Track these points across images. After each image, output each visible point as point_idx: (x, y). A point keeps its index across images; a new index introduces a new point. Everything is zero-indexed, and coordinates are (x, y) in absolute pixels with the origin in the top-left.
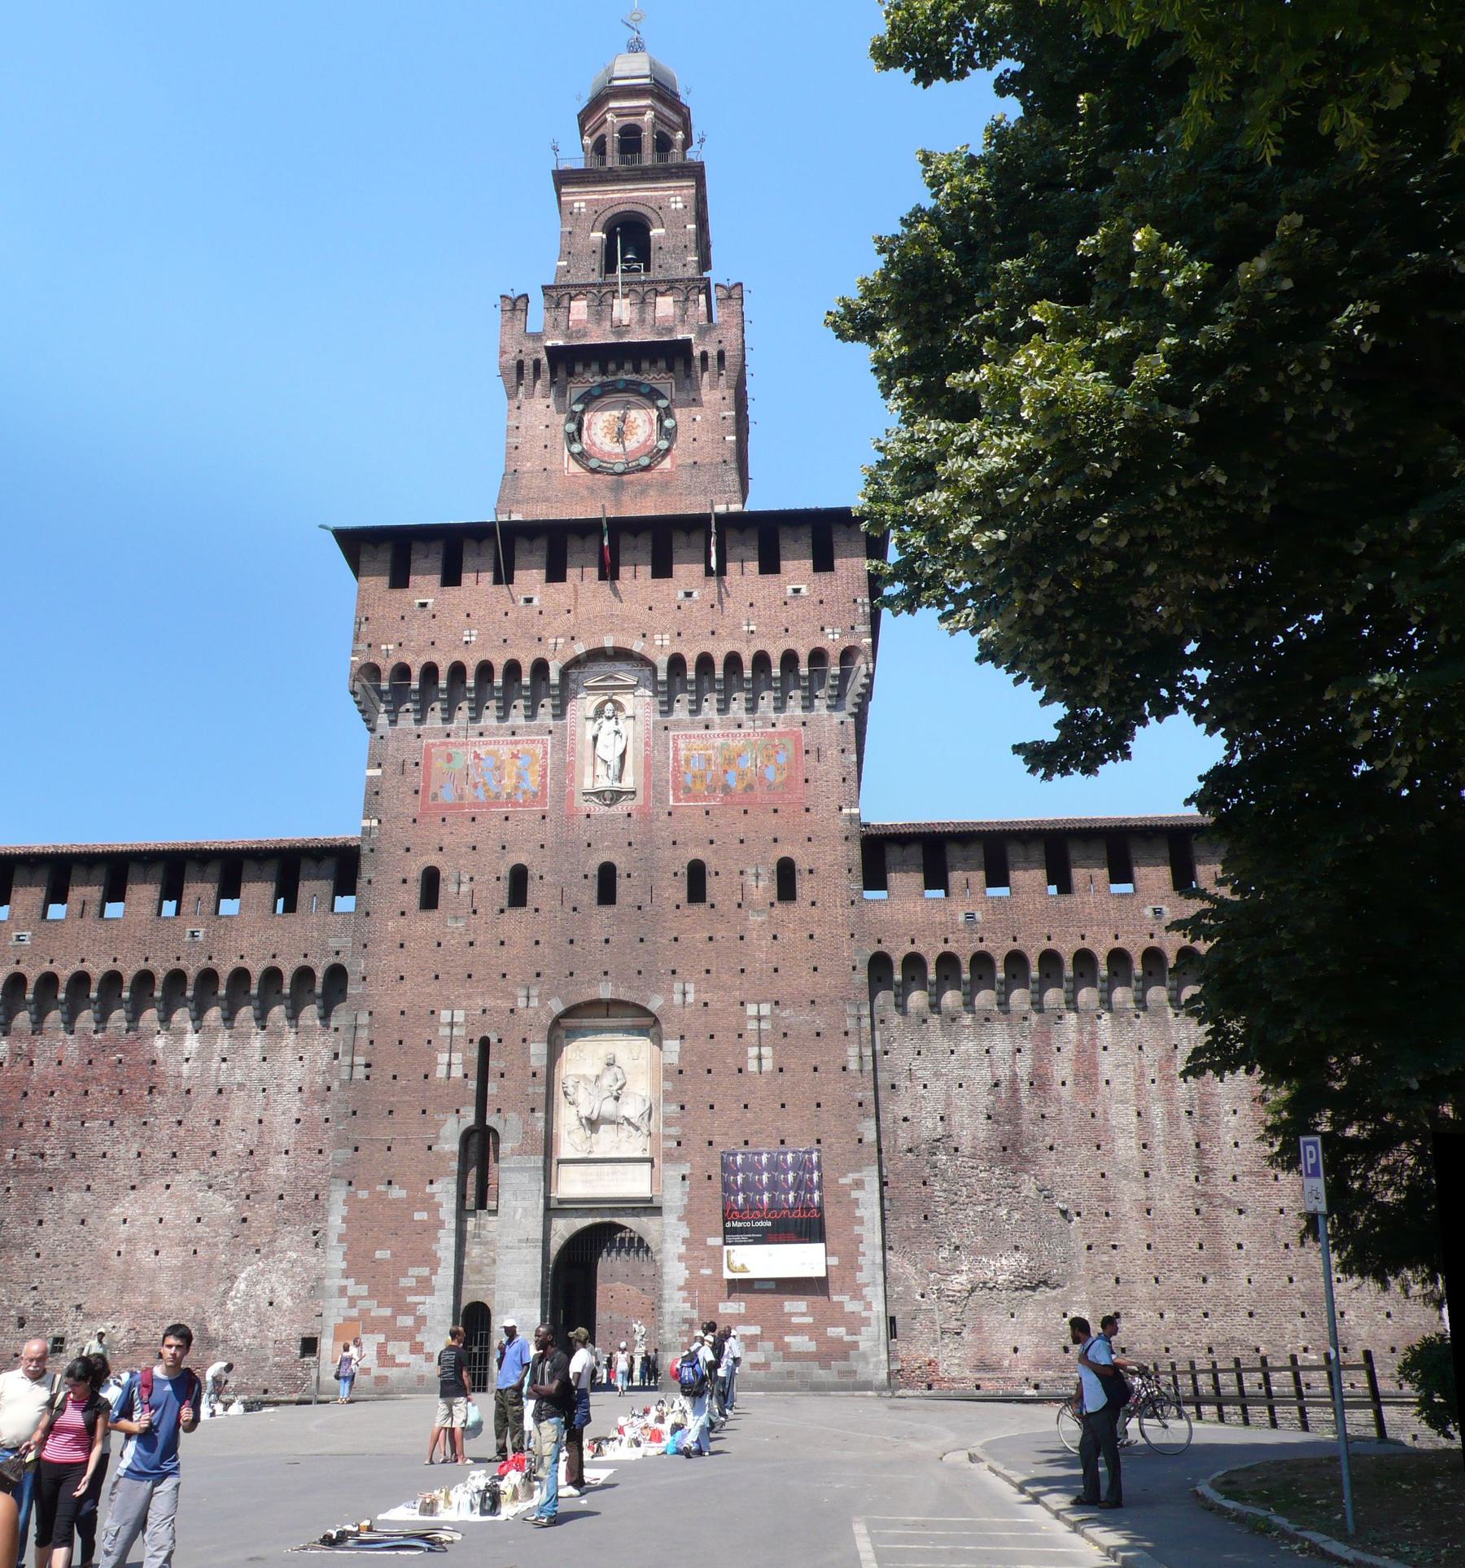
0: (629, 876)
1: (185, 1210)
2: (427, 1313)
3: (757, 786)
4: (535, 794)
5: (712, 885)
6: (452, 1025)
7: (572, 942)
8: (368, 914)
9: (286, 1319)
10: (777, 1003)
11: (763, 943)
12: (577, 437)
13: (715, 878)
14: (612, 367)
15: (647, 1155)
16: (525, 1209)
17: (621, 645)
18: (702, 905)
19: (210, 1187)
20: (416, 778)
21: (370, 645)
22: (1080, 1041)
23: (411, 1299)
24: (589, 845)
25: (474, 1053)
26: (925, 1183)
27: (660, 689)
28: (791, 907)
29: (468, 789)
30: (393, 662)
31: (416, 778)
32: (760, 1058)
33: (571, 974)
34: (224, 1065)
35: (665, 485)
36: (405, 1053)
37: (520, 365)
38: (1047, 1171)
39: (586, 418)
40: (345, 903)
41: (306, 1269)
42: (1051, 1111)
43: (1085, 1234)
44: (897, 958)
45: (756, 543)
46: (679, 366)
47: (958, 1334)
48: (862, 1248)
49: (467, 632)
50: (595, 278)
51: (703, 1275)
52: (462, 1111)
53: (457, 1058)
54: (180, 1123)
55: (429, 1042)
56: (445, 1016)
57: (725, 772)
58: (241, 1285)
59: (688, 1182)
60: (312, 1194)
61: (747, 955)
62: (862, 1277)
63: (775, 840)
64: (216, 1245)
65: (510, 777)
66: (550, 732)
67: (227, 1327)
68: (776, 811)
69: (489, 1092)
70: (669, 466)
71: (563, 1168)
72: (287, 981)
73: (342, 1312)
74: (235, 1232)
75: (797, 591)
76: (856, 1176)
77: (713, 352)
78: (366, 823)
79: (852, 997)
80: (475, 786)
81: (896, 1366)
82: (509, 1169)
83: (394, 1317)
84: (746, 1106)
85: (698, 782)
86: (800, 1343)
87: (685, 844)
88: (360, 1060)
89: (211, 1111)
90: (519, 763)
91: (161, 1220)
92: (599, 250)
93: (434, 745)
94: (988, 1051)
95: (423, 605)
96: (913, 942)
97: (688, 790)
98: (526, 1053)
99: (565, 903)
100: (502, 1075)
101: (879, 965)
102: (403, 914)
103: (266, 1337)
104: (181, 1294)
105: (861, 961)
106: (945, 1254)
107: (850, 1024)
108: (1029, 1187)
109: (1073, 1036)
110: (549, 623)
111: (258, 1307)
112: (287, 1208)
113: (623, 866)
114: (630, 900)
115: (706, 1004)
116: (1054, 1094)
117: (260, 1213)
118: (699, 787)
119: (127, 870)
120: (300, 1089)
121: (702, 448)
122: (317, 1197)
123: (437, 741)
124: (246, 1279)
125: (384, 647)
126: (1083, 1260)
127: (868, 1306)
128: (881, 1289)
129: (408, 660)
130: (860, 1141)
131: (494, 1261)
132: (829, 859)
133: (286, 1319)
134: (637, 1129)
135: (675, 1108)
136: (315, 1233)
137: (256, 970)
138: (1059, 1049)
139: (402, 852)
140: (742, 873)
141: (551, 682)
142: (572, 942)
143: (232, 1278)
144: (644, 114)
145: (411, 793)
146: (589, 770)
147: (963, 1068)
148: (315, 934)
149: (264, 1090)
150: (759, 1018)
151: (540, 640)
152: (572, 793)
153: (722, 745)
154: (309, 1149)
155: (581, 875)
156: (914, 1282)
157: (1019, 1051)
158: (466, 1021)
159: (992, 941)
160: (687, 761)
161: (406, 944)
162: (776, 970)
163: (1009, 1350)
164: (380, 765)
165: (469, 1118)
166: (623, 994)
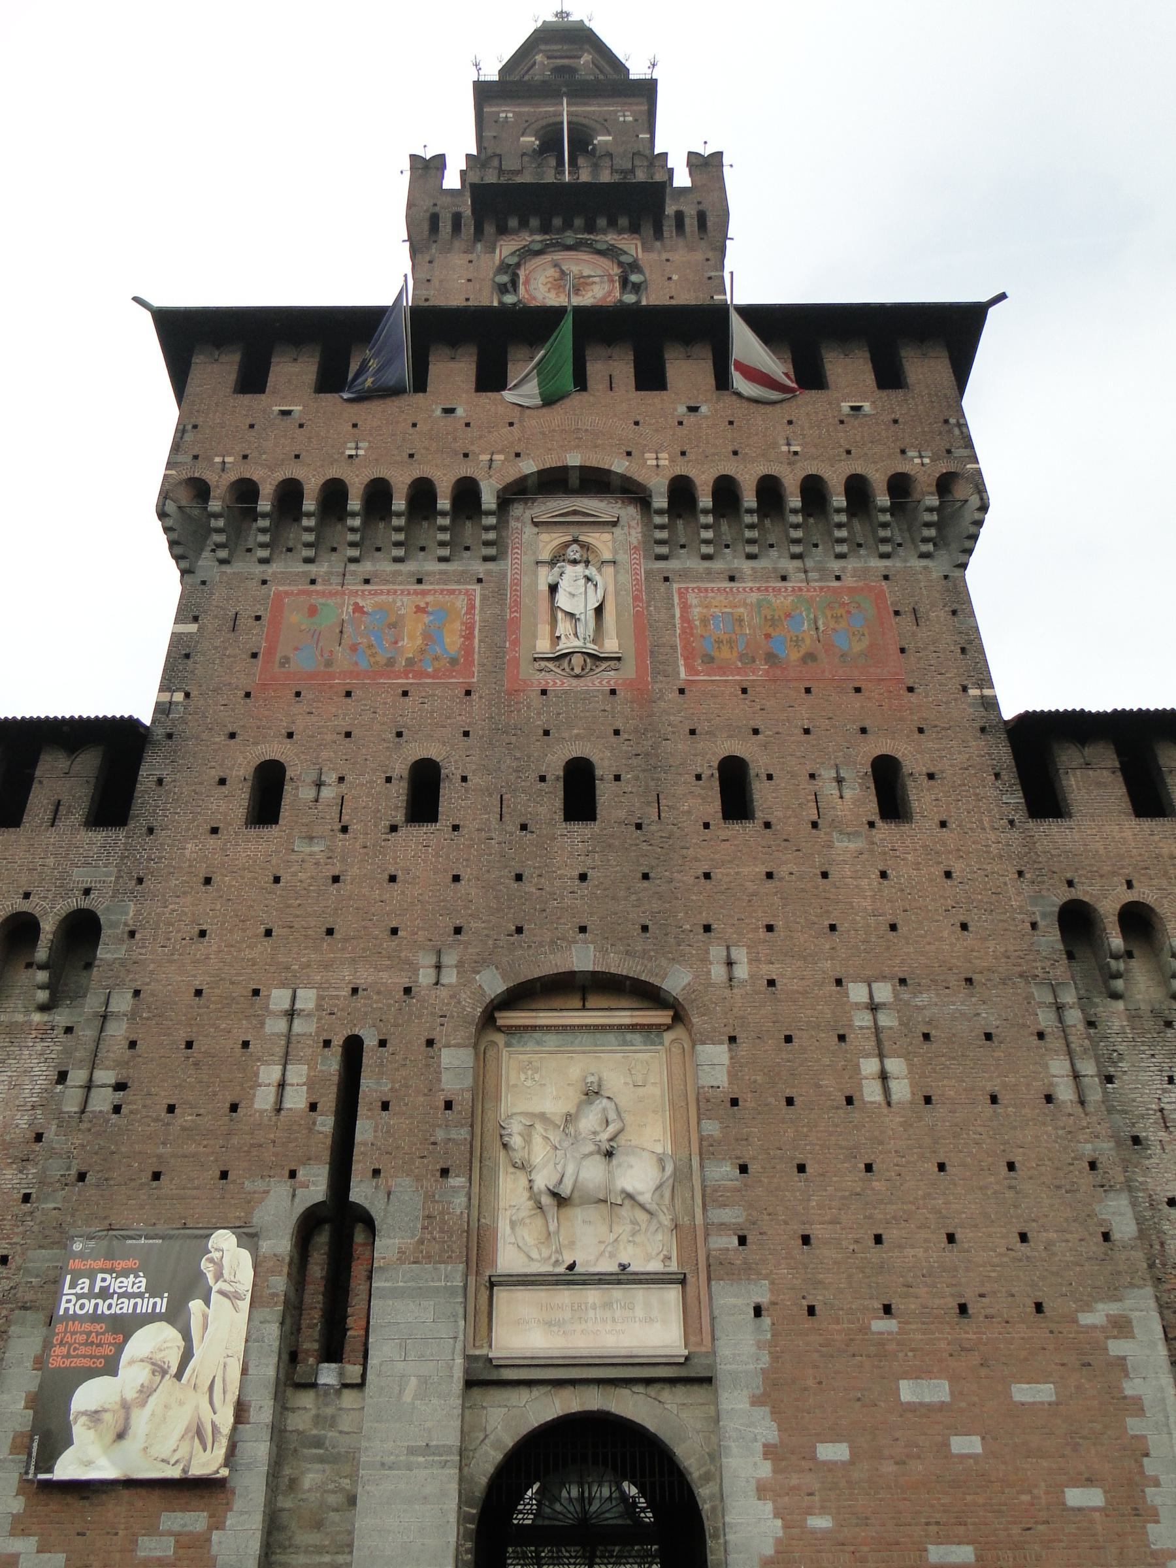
0: (617, 778)
4: (454, 661)
5: (762, 795)
6: (291, 1014)
7: (519, 878)
8: (151, 831)
10: (903, 981)
11: (864, 883)
13: (767, 783)
14: (557, 222)
15: (674, 1267)
16: (424, 1381)
17: (594, 464)
18: (749, 825)
20: (254, 637)
21: (196, 457)
25: (332, 1064)
27: (658, 520)
28: (905, 828)
29: (340, 653)
30: (232, 476)
31: (254, 637)
32: (884, 1076)
33: (519, 930)
36: (196, 1064)
39: (522, 273)
44: (1108, 907)
46: (648, 230)
48: (1150, 1467)
51: (813, 1532)
52: (301, 1174)
53: (298, 1073)
55: (246, 1044)
56: (279, 998)
57: (768, 636)
59: (766, 1321)
65: (412, 638)
66: (480, 581)
68: (858, 690)
69: (359, 1137)
76: (1113, 1308)
77: (690, 211)
78: (166, 697)
79: (1039, 972)
80: (354, 648)
82: (397, 1294)
84: (869, 1168)
85: (725, 648)
88: (106, 1076)
90: (427, 619)
93: (287, 593)
96: (1129, 884)
97: (709, 659)
98: (432, 1068)
99: (506, 817)
100: (385, 1106)
102: (215, 831)
105: (1044, 915)
107: (1046, 1019)
113: (606, 763)
114: (622, 814)
118: (725, 654)
123: (295, 589)
129: (255, 473)
130: (1106, 1237)
131: (352, 1501)
135: (724, 1172)
139: (221, 739)
140: (812, 776)
141: (484, 507)
144: (580, 57)
146: (544, 629)
148: (51, 861)
151: (466, 455)
152: (516, 662)
155: (535, 776)
158: (319, 1007)
160: (705, 621)
161: (216, 878)
162: (893, 927)
164: (196, 619)
166: (617, 964)
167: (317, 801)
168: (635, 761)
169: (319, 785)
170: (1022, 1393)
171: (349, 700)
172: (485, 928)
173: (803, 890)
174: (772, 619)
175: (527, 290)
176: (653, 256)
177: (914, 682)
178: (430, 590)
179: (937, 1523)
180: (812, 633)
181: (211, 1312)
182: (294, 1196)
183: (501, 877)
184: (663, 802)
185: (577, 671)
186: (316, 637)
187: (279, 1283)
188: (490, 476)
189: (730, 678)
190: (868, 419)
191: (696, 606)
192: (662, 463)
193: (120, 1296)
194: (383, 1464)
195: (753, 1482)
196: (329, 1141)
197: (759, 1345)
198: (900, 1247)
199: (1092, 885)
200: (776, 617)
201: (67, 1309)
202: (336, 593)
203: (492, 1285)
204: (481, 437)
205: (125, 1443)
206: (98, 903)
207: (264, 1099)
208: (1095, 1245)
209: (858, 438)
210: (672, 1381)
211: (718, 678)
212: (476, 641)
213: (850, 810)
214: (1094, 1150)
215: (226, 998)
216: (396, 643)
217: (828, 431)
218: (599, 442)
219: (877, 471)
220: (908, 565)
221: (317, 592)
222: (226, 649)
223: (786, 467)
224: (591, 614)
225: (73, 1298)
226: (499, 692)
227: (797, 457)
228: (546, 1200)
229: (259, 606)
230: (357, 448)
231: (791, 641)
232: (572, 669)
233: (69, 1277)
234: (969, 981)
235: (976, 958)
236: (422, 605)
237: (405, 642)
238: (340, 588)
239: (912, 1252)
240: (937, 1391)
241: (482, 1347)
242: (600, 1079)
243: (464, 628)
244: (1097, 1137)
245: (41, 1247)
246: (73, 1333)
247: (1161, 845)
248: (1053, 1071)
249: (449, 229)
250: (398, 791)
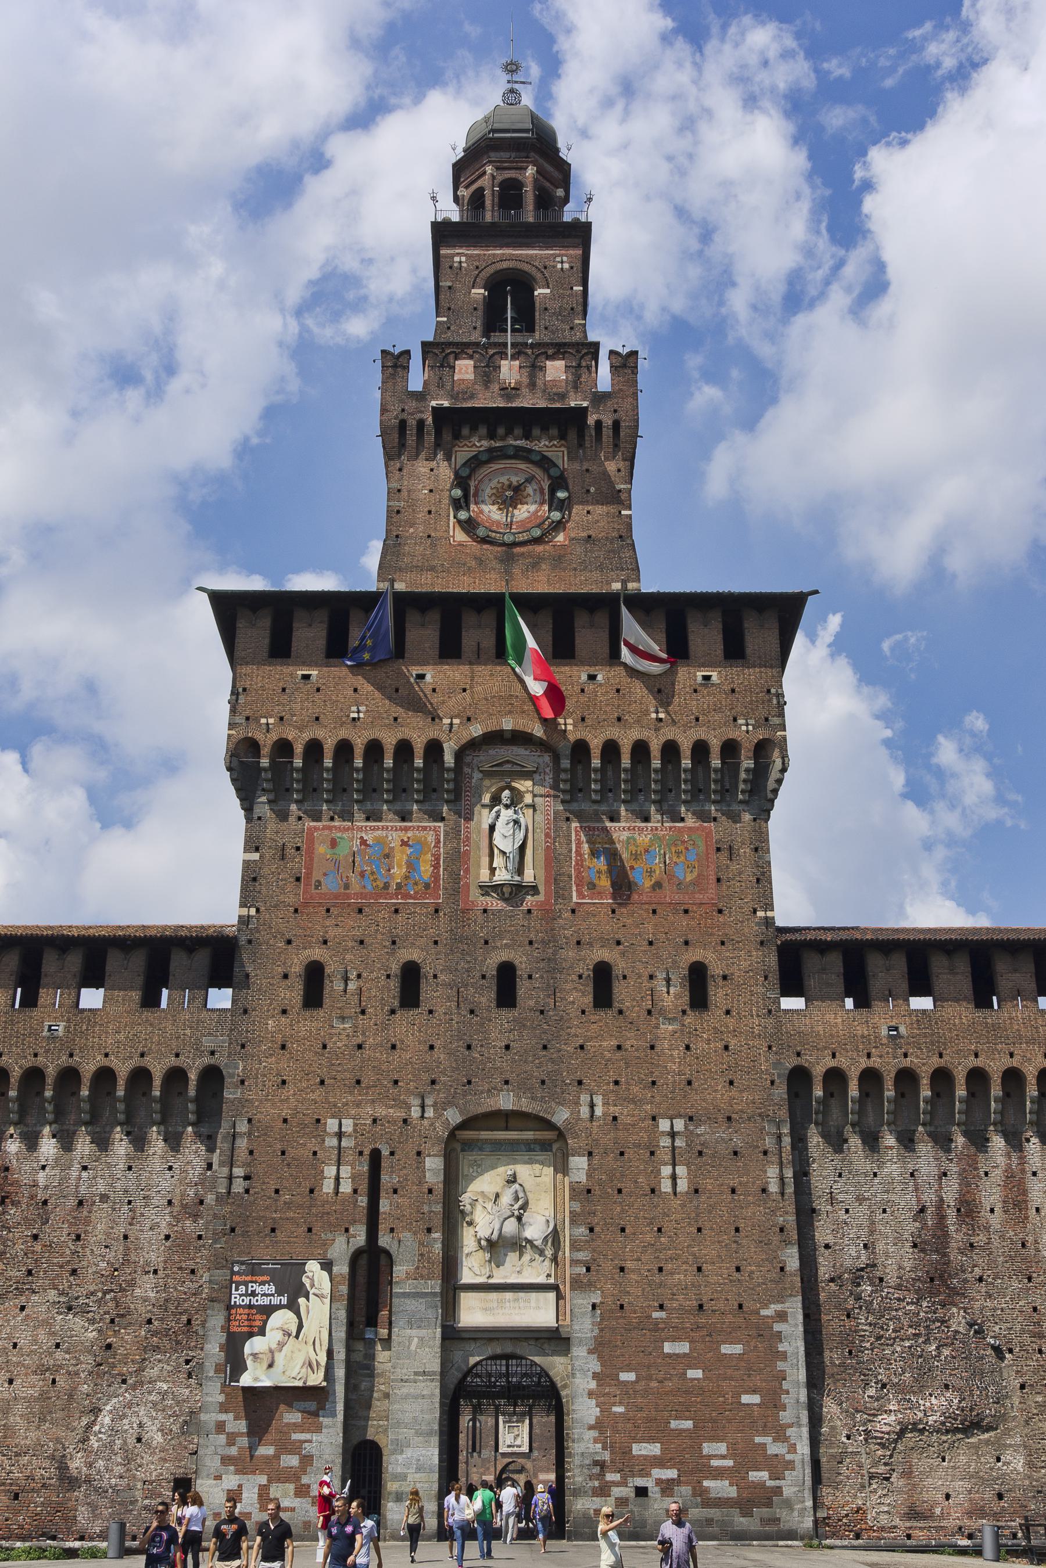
0: (530, 977)
1: (42, 1335)
2: (314, 1451)
3: (666, 884)
4: (427, 886)
6: (340, 1135)
8: (245, 1011)
9: (156, 1457)
10: (691, 1119)
12: (463, 504)
14: (501, 431)
15: (552, 1281)
16: (421, 1339)
17: (521, 728)
19: (70, 1308)
20: (297, 864)
21: (248, 718)
22: (1009, 1166)
23: (296, 1437)
24: (486, 942)
26: (848, 1316)
28: (705, 1015)
29: (354, 879)
30: (274, 736)
31: (297, 864)
32: (674, 1177)
33: (469, 1082)
34: (84, 1174)
35: (559, 560)
37: (403, 425)
38: (977, 1305)
39: (472, 484)
40: (221, 998)
41: (178, 1403)
42: (980, 1239)
43: (1017, 1372)
44: (818, 1071)
45: (663, 626)
47: (887, 1479)
48: (785, 1385)
49: (354, 708)
50: (476, 336)
52: (351, 1230)
53: (346, 1171)
54: (35, 1237)
55: (315, 1153)
56: (332, 1125)
58: (106, 1419)
60: (184, 1318)
61: (658, 1066)
62: (785, 1417)
63: (686, 943)
64: (77, 1374)
65: (400, 866)
67: (90, 1465)
68: (686, 911)
69: (382, 1210)
70: (562, 540)
71: (463, 1295)
72: (157, 1082)
73: (220, 1451)
74: (98, 1359)
75: (707, 678)
76: (779, 1307)
77: (608, 421)
78: (244, 911)
79: (771, 1113)
80: (362, 874)
81: (822, 1514)
83: (277, 1457)
84: (659, 1230)
86: (720, 1488)
87: (591, 944)
88: (238, 1171)
89: (71, 1224)
90: (409, 851)
91: (15, 1345)
92: (481, 307)
93: (316, 829)
94: (912, 1175)
95: (306, 677)
96: (834, 1056)
97: (592, 886)
98: (420, 1167)
99: (462, 1005)
100: (395, 1191)
101: (799, 1077)
102: (284, 1012)
103: (134, 1476)
104: (38, 1428)
106: (871, 1392)
107: (769, 1142)
108: (958, 1322)
109: (1001, 1160)
110: (443, 702)
111: (125, 1443)
112: (155, 1333)
114: (532, 1003)
115: (615, 1118)
116: (983, 1221)
117: (127, 1339)
119: (41, 959)
120: (170, 1202)
121: (597, 521)
122: (189, 1321)
124: (111, 1412)
125: (263, 721)
126: (1016, 1401)
127: (792, 1449)
128: (805, 1431)
129: (291, 735)
130: (782, 1269)
132: (744, 964)
133: (156, 1457)
134: (541, 1253)
135: (583, 1230)
136: (187, 1362)
137: (123, 1070)
138: (986, 1174)
140: (651, 977)
141: (446, 765)
142: (469, 1047)
143: (96, 1411)
146: (485, 860)
147: (887, 1192)
148: (188, 1032)
149: (130, 1202)
150: (673, 1135)
152: (467, 885)
153: (628, 838)
154: (180, 1268)
155: (478, 975)
156: (839, 1423)
157: (945, 1174)
158: (355, 1131)
159: (917, 1057)
163: (940, 1497)
164: (257, 849)
165: (360, 1238)
166: (526, 1105)
167: (345, 991)
168: (542, 965)
169: (346, 980)
170: (726, 1349)
172: (449, 1081)
173: (638, 1058)
176: (576, 466)
178: (410, 827)
179: (676, 1411)
181: (310, 1304)
182: (348, 1242)
183: (459, 1046)
184: (558, 995)
185: (507, 895)
187: (344, 1289)
189: (605, 901)
193: (262, 1295)
194: (402, 1380)
195: (586, 1390)
196: (365, 1211)
197: (593, 1324)
198: (672, 1274)
199: (811, 1055)
201: (235, 1302)
202: (348, 829)
203: (455, 1289)
205: (272, 1369)
206: (220, 1060)
207: (328, 1187)
208: (775, 1274)
210: (549, 1339)
211: (597, 901)
212: (441, 869)
213: (672, 1002)
214: (784, 1221)
215: (301, 1124)
216: (389, 870)
217: (685, 699)
219: (715, 737)
221: (335, 827)
222: (279, 874)
224: (516, 852)
225: (238, 1296)
226: (456, 910)
228: (483, 1243)
230: (358, 712)
231: (647, 872)
232: (503, 894)
233: (234, 1285)
234: (729, 1119)
235: (736, 1104)
236: (406, 839)
237: (395, 871)
239: (677, 1276)
240: (683, 1348)
241: (450, 1321)
242: (515, 1174)
244: (787, 1213)
245: (216, 1269)
246: (240, 1315)
247: (858, 1028)
248: (769, 1175)
250: (394, 985)
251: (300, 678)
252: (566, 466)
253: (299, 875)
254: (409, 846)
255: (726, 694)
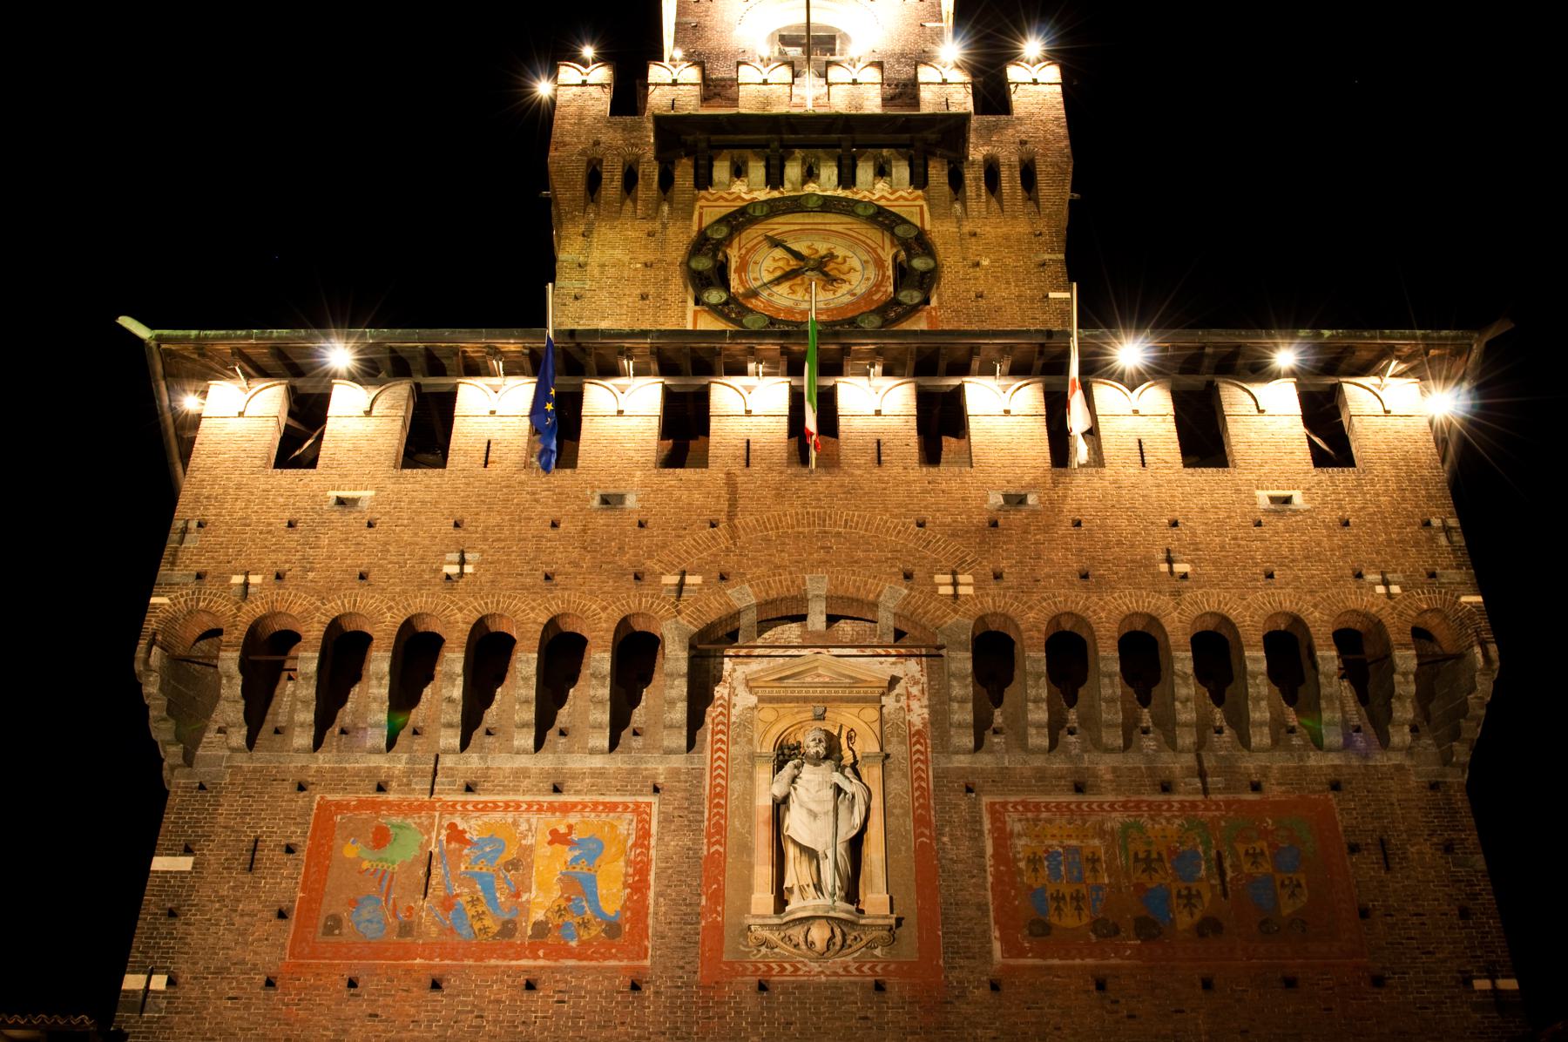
4: (613, 929)
39: (734, 255)
90: (569, 854)
93: (339, 806)
97: (1041, 929)
118: (1069, 920)
145: (270, 914)
146: (763, 873)
153: (1126, 827)
160: (1034, 861)
164: (188, 851)
171: (437, 995)
174: (1148, 860)
175: (742, 282)
177: (1384, 968)
178: (575, 805)
180: (1213, 882)
186: (385, 884)
188: (679, 612)
189: (1078, 961)
190: (1299, 518)
191: (1019, 835)
192: (962, 590)
200: (1154, 856)
204: (664, 546)
209: (1285, 552)
211: (1056, 962)
216: (518, 895)
218: (860, 554)
219: (1315, 606)
220: (1371, 763)
221: (389, 804)
222: (238, 901)
223: (1167, 598)
227: (1186, 583)
229: (293, 829)
231: (1179, 896)
236: (563, 829)
238: (426, 798)
243: (631, 871)
249: (617, 183)
251: (332, 501)
252: (927, 227)
253: (284, 905)
254: (571, 843)
255: (1327, 527)
